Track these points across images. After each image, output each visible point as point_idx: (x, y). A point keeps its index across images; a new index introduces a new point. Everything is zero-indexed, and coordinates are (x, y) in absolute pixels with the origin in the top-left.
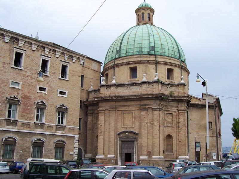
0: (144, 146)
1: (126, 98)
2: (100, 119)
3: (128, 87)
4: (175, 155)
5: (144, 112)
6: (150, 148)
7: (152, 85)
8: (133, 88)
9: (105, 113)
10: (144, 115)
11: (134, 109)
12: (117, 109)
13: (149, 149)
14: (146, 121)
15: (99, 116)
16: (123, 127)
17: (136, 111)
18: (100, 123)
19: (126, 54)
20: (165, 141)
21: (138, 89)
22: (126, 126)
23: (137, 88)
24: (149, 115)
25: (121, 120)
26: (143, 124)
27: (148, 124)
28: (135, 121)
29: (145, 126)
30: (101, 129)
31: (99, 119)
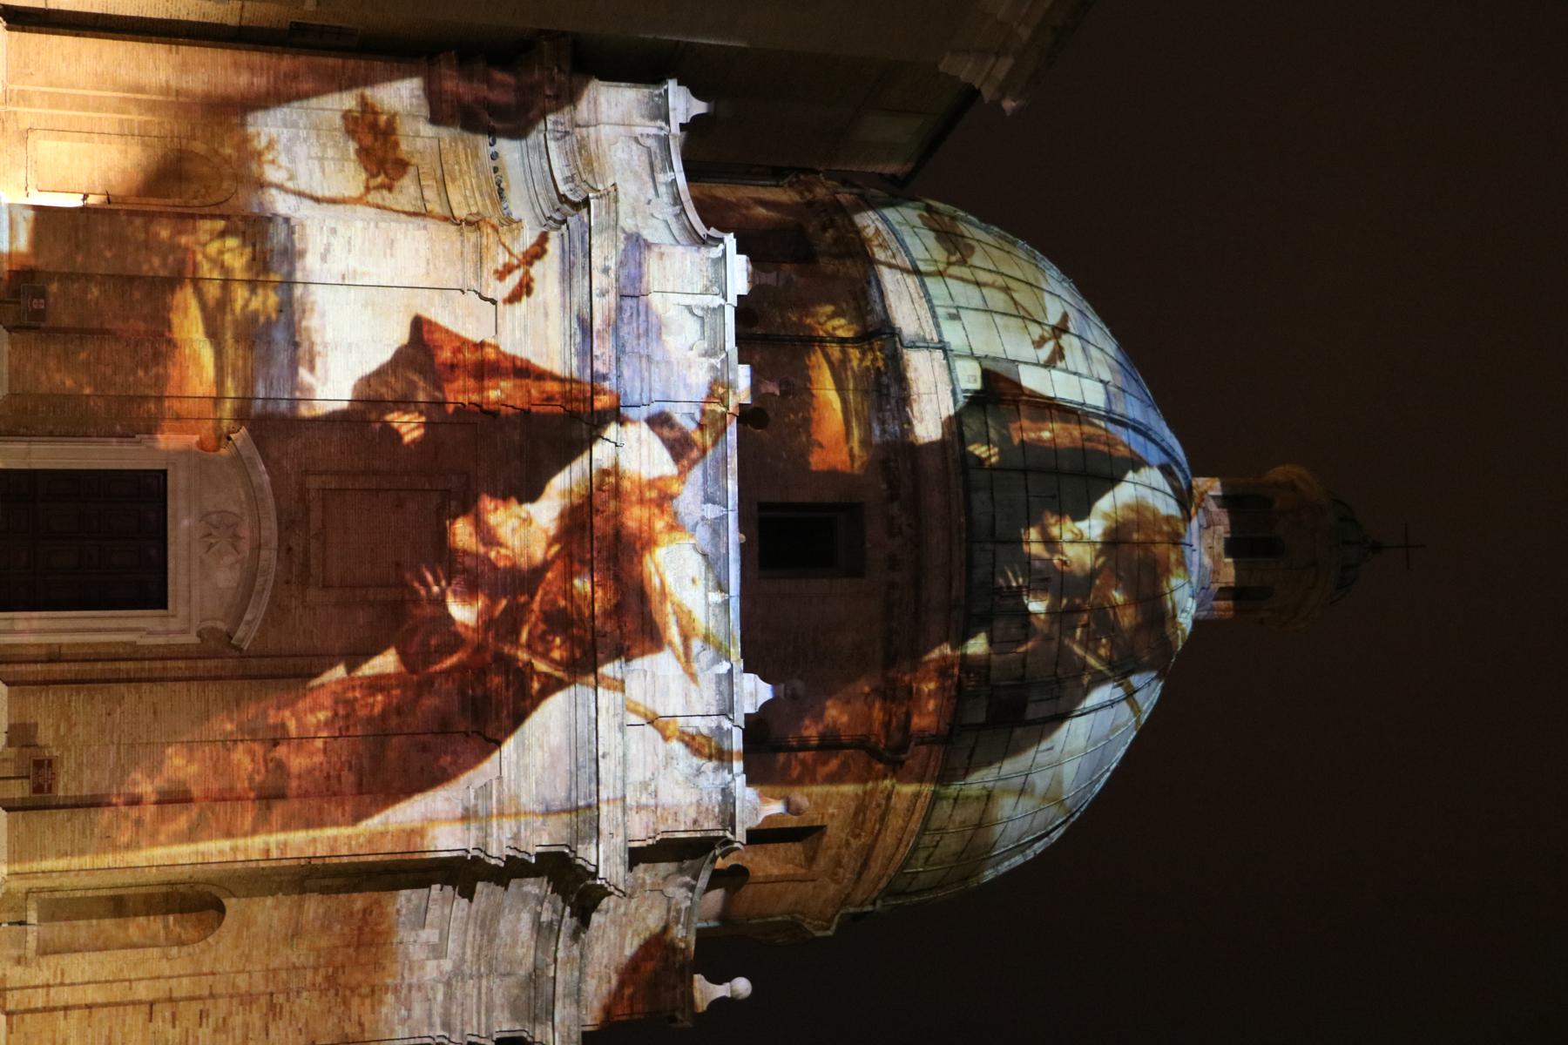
0: (117, 715)
4: (19, 970)
6: (87, 774)
13: (80, 765)
16: (314, 483)
18: (357, 242)
20: (164, 889)
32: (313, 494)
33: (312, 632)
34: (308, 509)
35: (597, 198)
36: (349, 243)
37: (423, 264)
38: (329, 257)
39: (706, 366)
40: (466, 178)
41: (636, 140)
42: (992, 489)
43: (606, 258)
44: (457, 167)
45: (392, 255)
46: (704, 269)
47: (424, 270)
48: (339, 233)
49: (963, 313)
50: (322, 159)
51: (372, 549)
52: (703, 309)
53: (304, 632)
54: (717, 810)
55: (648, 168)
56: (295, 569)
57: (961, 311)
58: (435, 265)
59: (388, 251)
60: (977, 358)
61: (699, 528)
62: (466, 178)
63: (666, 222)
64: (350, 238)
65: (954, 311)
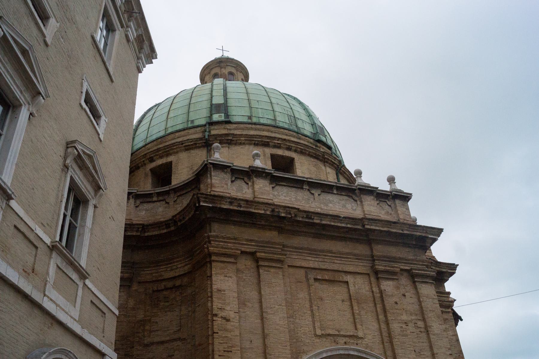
1: (324, 222)
2: (219, 290)
3: (316, 192)
5: (390, 283)
7: (389, 203)
8: (330, 202)
9: (238, 270)
10: (392, 296)
11: (351, 269)
12: (289, 262)
14: (405, 317)
15: (214, 278)
16: (319, 332)
17: (358, 277)
18: (220, 306)
19: (250, 117)
21: (349, 206)
22: (331, 332)
23: (343, 202)
24: (404, 295)
25: (307, 305)
26: (395, 327)
27: (411, 328)
28: (363, 312)
29: (407, 336)
30: (229, 335)
31: (214, 287)
32: (323, 332)
33: (373, 336)
34: (329, 335)
35: (199, 203)
36: (221, 309)
37: (227, 278)
38: (228, 318)
39: (255, 179)
40: (160, 270)
41: (137, 207)
42: (259, 117)
43: (226, 202)
44: (154, 275)
45: (224, 291)
46: (218, 173)
47: (230, 278)
48: (216, 313)
49: (190, 119)
50: (151, 332)
51: (339, 310)
52: (232, 177)
53: (374, 339)
54: (402, 202)
55: (150, 204)
56: (352, 341)
57: (190, 119)
58: (227, 274)
59: (222, 292)
60: (211, 115)
61: (312, 192)
62: (160, 270)
63: (178, 196)
64: (218, 308)
65: (189, 122)
